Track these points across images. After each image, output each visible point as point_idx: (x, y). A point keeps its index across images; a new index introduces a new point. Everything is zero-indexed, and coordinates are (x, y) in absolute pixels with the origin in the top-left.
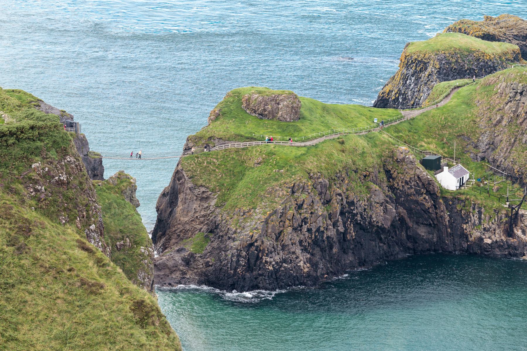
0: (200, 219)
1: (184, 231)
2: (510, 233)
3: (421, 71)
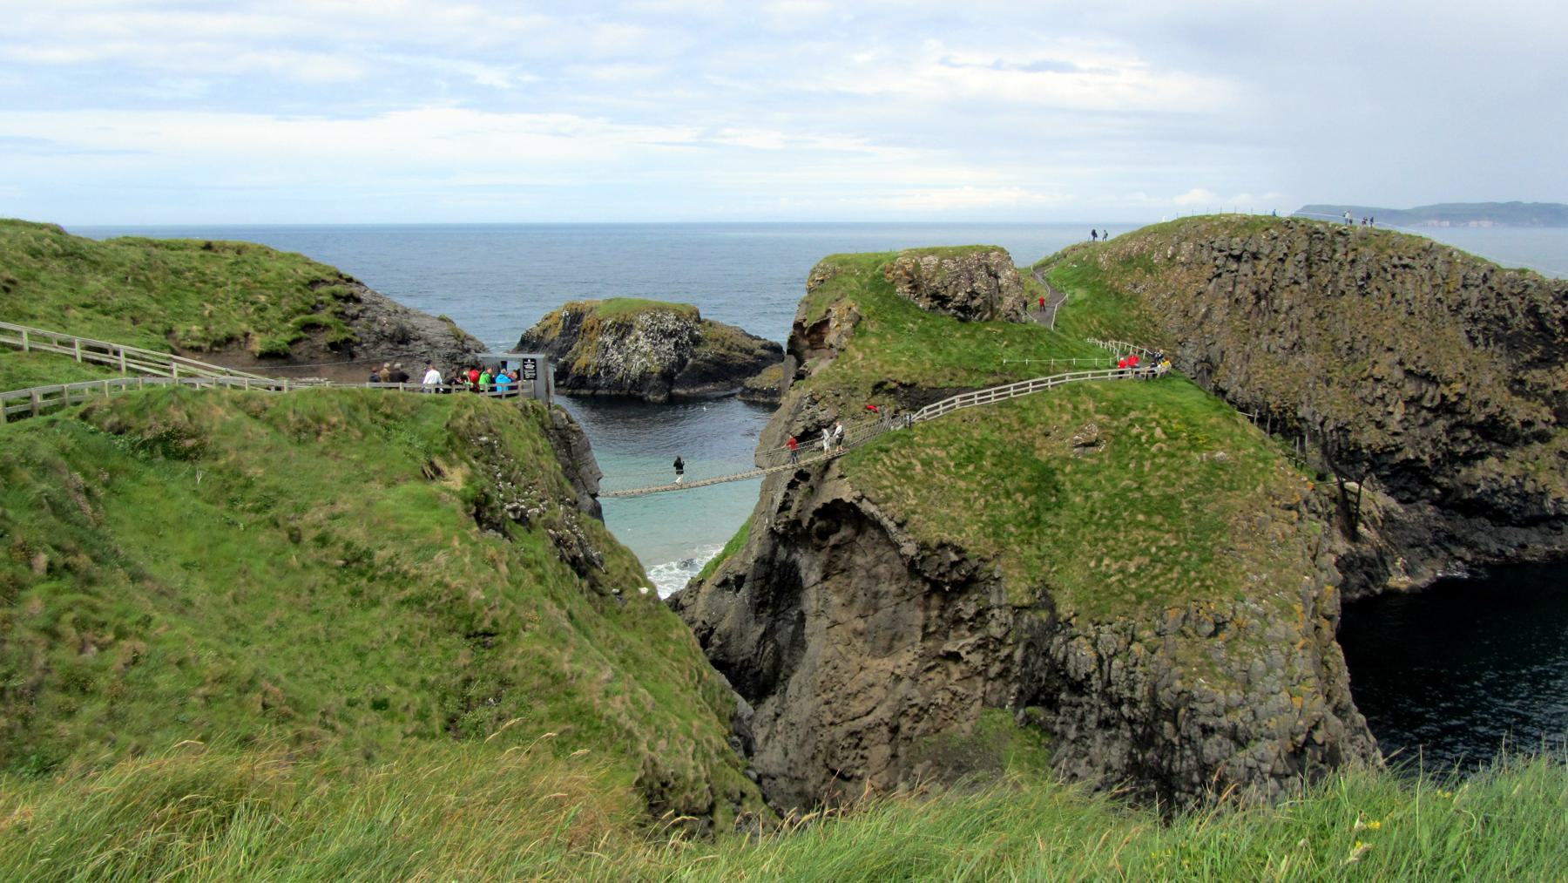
1: (915, 710)
2: (1354, 536)
3: (622, 337)
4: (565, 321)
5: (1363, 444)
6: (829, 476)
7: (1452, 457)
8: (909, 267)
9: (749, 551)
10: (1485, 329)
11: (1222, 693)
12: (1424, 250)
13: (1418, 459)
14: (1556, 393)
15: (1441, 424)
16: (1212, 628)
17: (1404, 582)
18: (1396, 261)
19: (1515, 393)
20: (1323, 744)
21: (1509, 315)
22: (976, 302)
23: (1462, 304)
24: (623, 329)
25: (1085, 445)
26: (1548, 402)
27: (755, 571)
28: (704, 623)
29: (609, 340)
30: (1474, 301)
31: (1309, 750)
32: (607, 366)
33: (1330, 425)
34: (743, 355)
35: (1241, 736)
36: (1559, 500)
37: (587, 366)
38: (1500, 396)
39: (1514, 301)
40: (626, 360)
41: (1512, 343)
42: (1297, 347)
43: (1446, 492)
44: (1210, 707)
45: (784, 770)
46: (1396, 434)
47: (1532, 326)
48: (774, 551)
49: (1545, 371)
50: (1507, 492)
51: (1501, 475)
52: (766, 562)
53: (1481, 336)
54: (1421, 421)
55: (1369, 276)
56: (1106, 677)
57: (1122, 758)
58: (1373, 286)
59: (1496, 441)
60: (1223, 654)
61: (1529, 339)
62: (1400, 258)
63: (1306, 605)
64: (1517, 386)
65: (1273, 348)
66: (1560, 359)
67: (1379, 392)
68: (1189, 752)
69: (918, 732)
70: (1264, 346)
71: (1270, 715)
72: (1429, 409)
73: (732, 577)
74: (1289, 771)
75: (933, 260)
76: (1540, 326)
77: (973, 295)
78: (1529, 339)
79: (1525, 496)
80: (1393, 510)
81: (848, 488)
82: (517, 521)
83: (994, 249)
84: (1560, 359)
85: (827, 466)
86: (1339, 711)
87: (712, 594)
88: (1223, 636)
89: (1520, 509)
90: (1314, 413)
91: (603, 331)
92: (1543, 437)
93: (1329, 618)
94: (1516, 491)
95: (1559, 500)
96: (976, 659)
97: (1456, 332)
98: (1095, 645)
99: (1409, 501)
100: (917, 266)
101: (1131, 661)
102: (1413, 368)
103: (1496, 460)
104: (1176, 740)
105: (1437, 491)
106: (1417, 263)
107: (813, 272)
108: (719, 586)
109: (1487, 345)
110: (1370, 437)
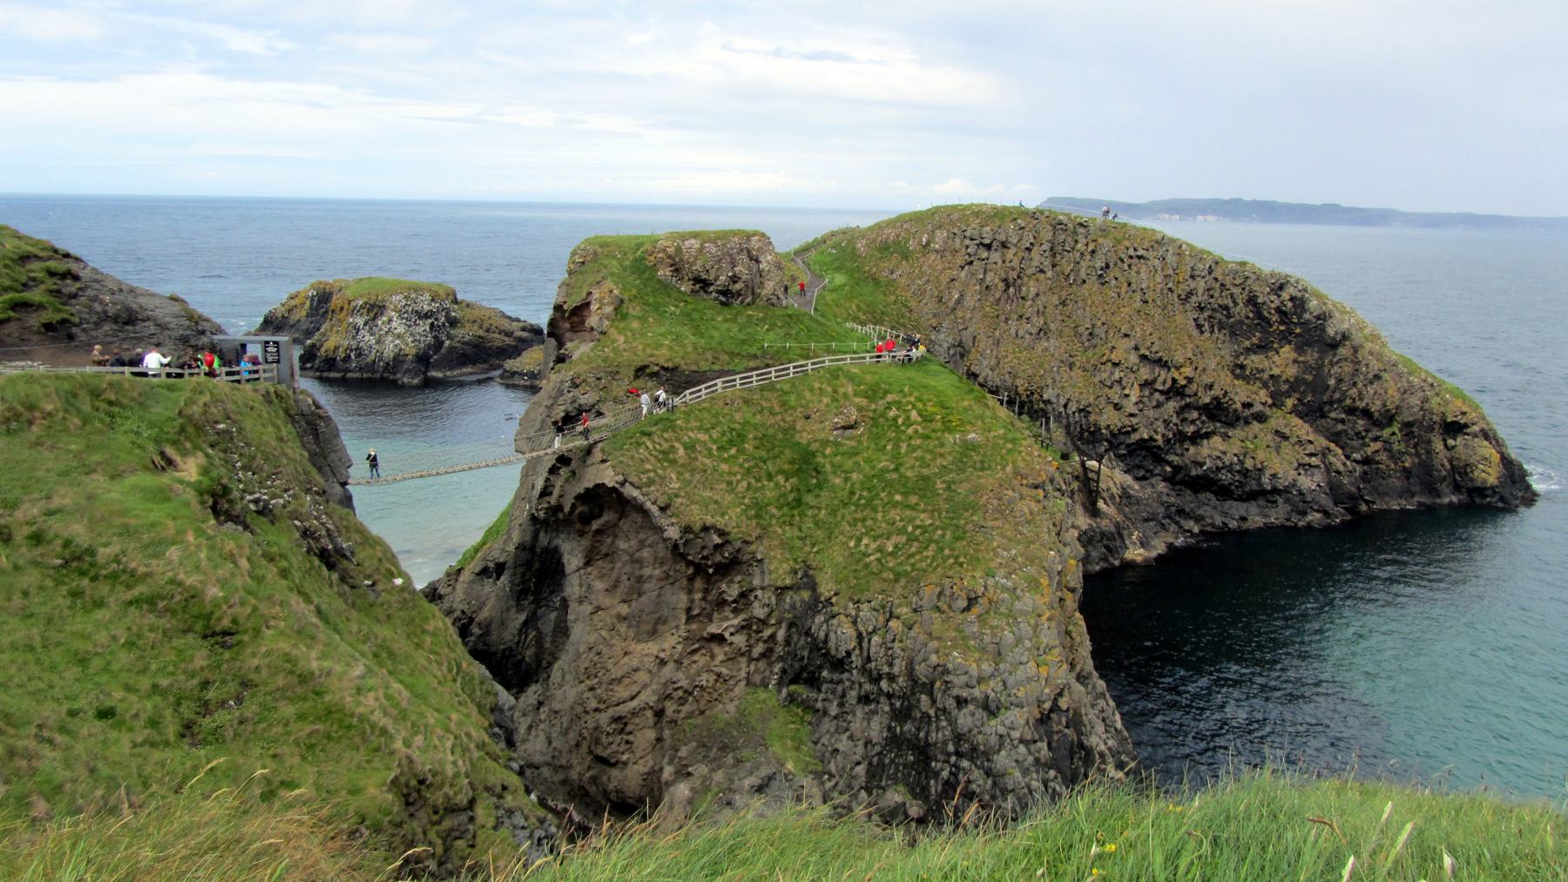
0: (733, 639)
1: (680, 693)
2: (1094, 512)
3: (375, 318)
4: (312, 300)
5: (1103, 425)
6: (590, 460)
7: (1181, 437)
8: (671, 250)
9: (509, 538)
10: (1210, 317)
11: (974, 665)
12: (1157, 242)
13: (1151, 439)
14: (1272, 376)
15: (1172, 405)
16: (965, 604)
17: (1140, 555)
18: (1131, 252)
19: (1237, 377)
20: (1068, 710)
21: (1231, 305)
22: (738, 286)
23: (1190, 294)
24: (375, 309)
25: (845, 428)
26: (1265, 386)
27: (516, 556)
28: (463, 612)
29: (360, 321)
30: (1200, 291)
31: (1054, 716)
33: (1073, 407)
34: (502, 337)
35: (993, 706)
36: (1274, 476)
37: (337, 348)
38: (1224, 380)
39: (1236, 291)
40: (378, 342)
41: (1234, 331)
42: (1043, 332)
43: (1177, 469)
44: (964, 679)
45: (548, 758)
46: (1132, 415)
47: (1251, 315)
48: (535, 537)
49: (1262, 356)
50: (1230, 468)
51: (1224, 453)
52: (528, 551)
53: (1206, 324)
54: (1154, 403)
55: (1107, 266)
56: (865, 654)
57: (881, 732)
58: (1112, 275)
59: (1220, 421)
60: (975, 629)
61: (1249, 326)
62: (1135, 250)
63: (1051, 578)
64: (1238, 370)
65: (1021, 333)
66: (1276, 345)
67: (1117, 376)
68: (944, 724)
69: (682, 715)
70: (1013, 331)
71: (1019, 684)
72: (1161, 392)
73: (492, 565)
74: (1037, 737)
75: (695, 243)
76: (1259, 314)
77: (734, 279)
78: (1249, 326)
79: (1245, 473)
80: (1129, 486)
81: (610, 472)
82: (259, 513)
83: (755, 234)
84: (1276, 345)
85: (589, 451)
86: (1081, 678)
87: (471, 583)
88: (976, 610)
89: (1241, 485)
90: (1058, 396)
91: (353, 312)
92: (1261, 418)
93: (1073, 590)
94: (1238, 468)
95: (1274, 476)
96: (740, 640)
97: (1185, 319)
98: (855, 623)
99: (1143, 478)
100: (679, 249)
101: (889, 637)
102: (1147, 353)
103: (1220, 440)
104: (932, 712)
105: (1168, 469)
106: (1150, 255)
107: (574, 254)
108: (478, 574)
109: (1212, 332)
110: (1108, 419)
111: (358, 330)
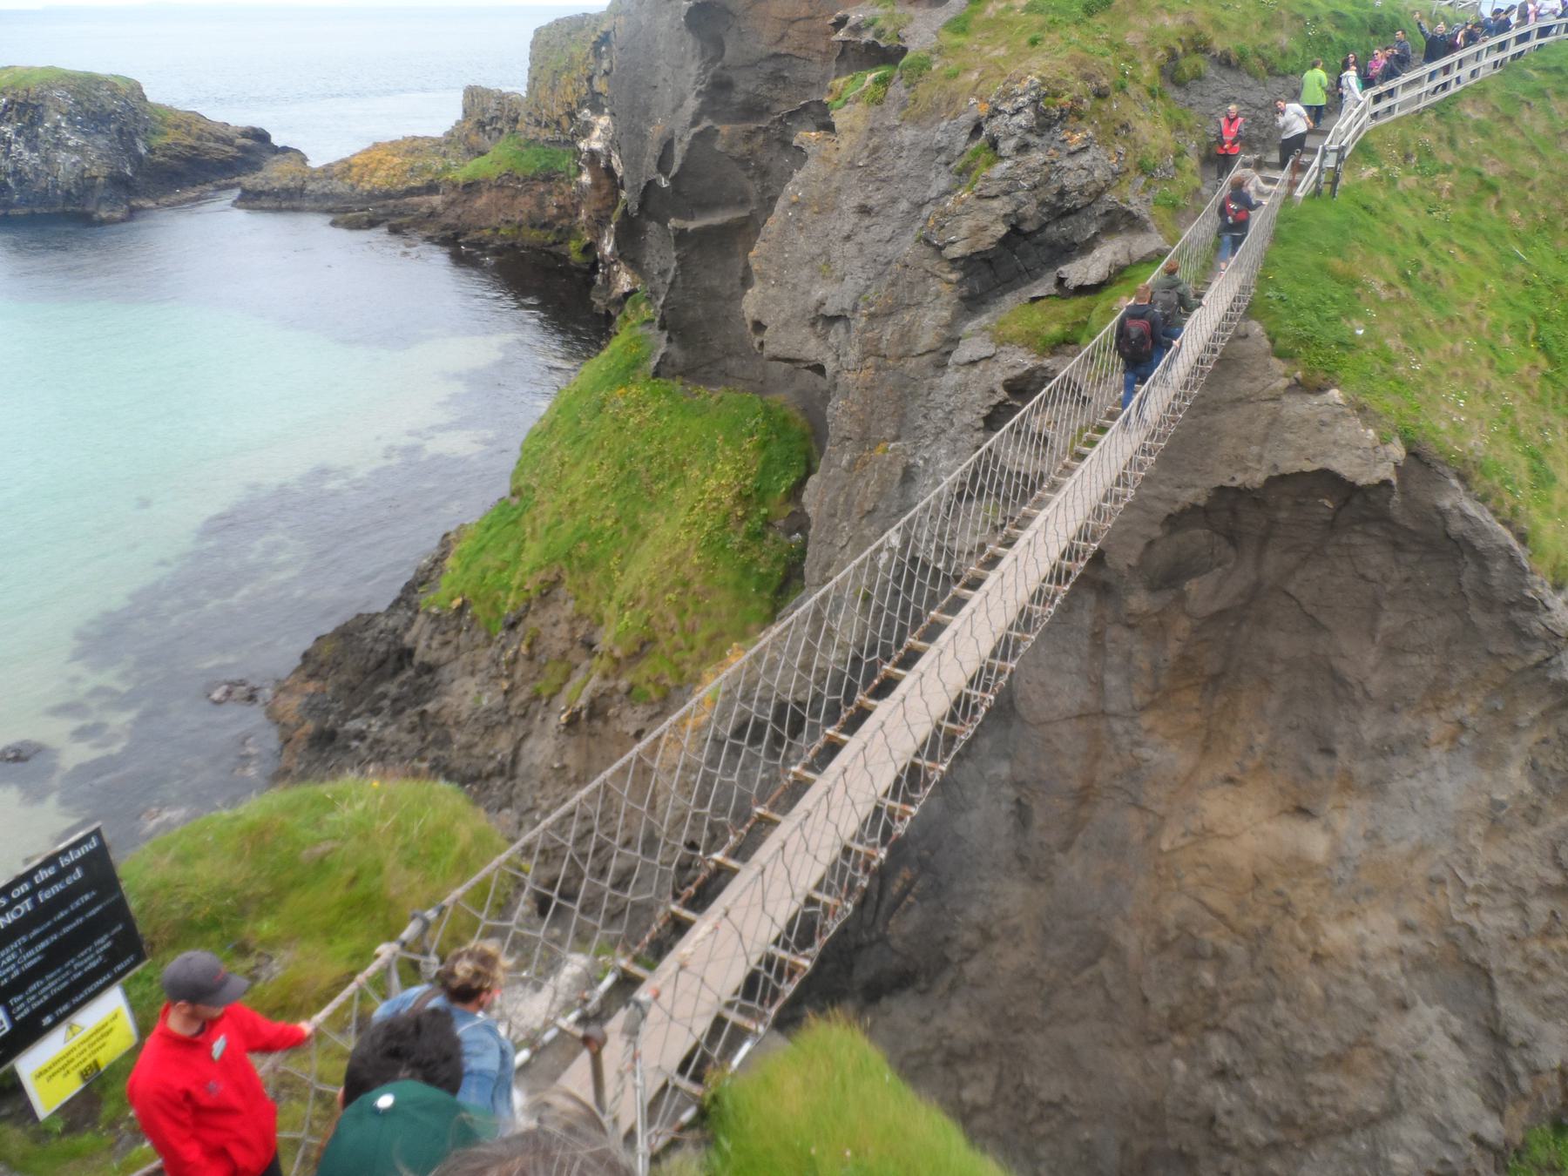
32: (16, 172)
34: (219, 146)
40: (46, 161)
111: (10, 143)
